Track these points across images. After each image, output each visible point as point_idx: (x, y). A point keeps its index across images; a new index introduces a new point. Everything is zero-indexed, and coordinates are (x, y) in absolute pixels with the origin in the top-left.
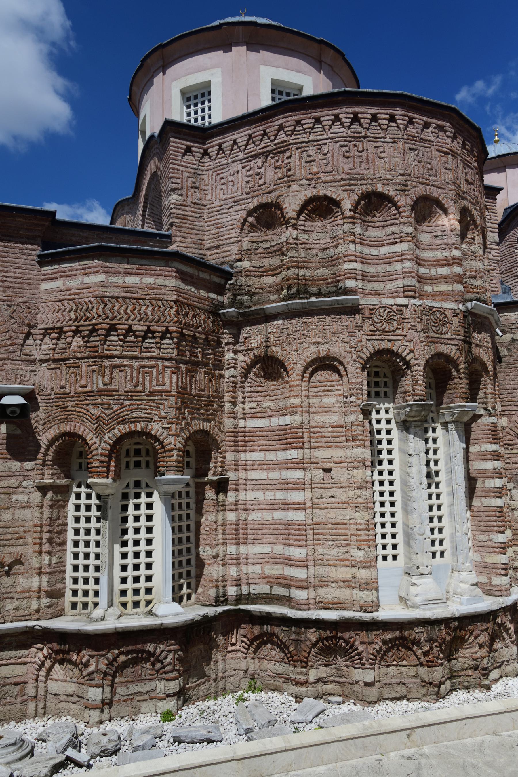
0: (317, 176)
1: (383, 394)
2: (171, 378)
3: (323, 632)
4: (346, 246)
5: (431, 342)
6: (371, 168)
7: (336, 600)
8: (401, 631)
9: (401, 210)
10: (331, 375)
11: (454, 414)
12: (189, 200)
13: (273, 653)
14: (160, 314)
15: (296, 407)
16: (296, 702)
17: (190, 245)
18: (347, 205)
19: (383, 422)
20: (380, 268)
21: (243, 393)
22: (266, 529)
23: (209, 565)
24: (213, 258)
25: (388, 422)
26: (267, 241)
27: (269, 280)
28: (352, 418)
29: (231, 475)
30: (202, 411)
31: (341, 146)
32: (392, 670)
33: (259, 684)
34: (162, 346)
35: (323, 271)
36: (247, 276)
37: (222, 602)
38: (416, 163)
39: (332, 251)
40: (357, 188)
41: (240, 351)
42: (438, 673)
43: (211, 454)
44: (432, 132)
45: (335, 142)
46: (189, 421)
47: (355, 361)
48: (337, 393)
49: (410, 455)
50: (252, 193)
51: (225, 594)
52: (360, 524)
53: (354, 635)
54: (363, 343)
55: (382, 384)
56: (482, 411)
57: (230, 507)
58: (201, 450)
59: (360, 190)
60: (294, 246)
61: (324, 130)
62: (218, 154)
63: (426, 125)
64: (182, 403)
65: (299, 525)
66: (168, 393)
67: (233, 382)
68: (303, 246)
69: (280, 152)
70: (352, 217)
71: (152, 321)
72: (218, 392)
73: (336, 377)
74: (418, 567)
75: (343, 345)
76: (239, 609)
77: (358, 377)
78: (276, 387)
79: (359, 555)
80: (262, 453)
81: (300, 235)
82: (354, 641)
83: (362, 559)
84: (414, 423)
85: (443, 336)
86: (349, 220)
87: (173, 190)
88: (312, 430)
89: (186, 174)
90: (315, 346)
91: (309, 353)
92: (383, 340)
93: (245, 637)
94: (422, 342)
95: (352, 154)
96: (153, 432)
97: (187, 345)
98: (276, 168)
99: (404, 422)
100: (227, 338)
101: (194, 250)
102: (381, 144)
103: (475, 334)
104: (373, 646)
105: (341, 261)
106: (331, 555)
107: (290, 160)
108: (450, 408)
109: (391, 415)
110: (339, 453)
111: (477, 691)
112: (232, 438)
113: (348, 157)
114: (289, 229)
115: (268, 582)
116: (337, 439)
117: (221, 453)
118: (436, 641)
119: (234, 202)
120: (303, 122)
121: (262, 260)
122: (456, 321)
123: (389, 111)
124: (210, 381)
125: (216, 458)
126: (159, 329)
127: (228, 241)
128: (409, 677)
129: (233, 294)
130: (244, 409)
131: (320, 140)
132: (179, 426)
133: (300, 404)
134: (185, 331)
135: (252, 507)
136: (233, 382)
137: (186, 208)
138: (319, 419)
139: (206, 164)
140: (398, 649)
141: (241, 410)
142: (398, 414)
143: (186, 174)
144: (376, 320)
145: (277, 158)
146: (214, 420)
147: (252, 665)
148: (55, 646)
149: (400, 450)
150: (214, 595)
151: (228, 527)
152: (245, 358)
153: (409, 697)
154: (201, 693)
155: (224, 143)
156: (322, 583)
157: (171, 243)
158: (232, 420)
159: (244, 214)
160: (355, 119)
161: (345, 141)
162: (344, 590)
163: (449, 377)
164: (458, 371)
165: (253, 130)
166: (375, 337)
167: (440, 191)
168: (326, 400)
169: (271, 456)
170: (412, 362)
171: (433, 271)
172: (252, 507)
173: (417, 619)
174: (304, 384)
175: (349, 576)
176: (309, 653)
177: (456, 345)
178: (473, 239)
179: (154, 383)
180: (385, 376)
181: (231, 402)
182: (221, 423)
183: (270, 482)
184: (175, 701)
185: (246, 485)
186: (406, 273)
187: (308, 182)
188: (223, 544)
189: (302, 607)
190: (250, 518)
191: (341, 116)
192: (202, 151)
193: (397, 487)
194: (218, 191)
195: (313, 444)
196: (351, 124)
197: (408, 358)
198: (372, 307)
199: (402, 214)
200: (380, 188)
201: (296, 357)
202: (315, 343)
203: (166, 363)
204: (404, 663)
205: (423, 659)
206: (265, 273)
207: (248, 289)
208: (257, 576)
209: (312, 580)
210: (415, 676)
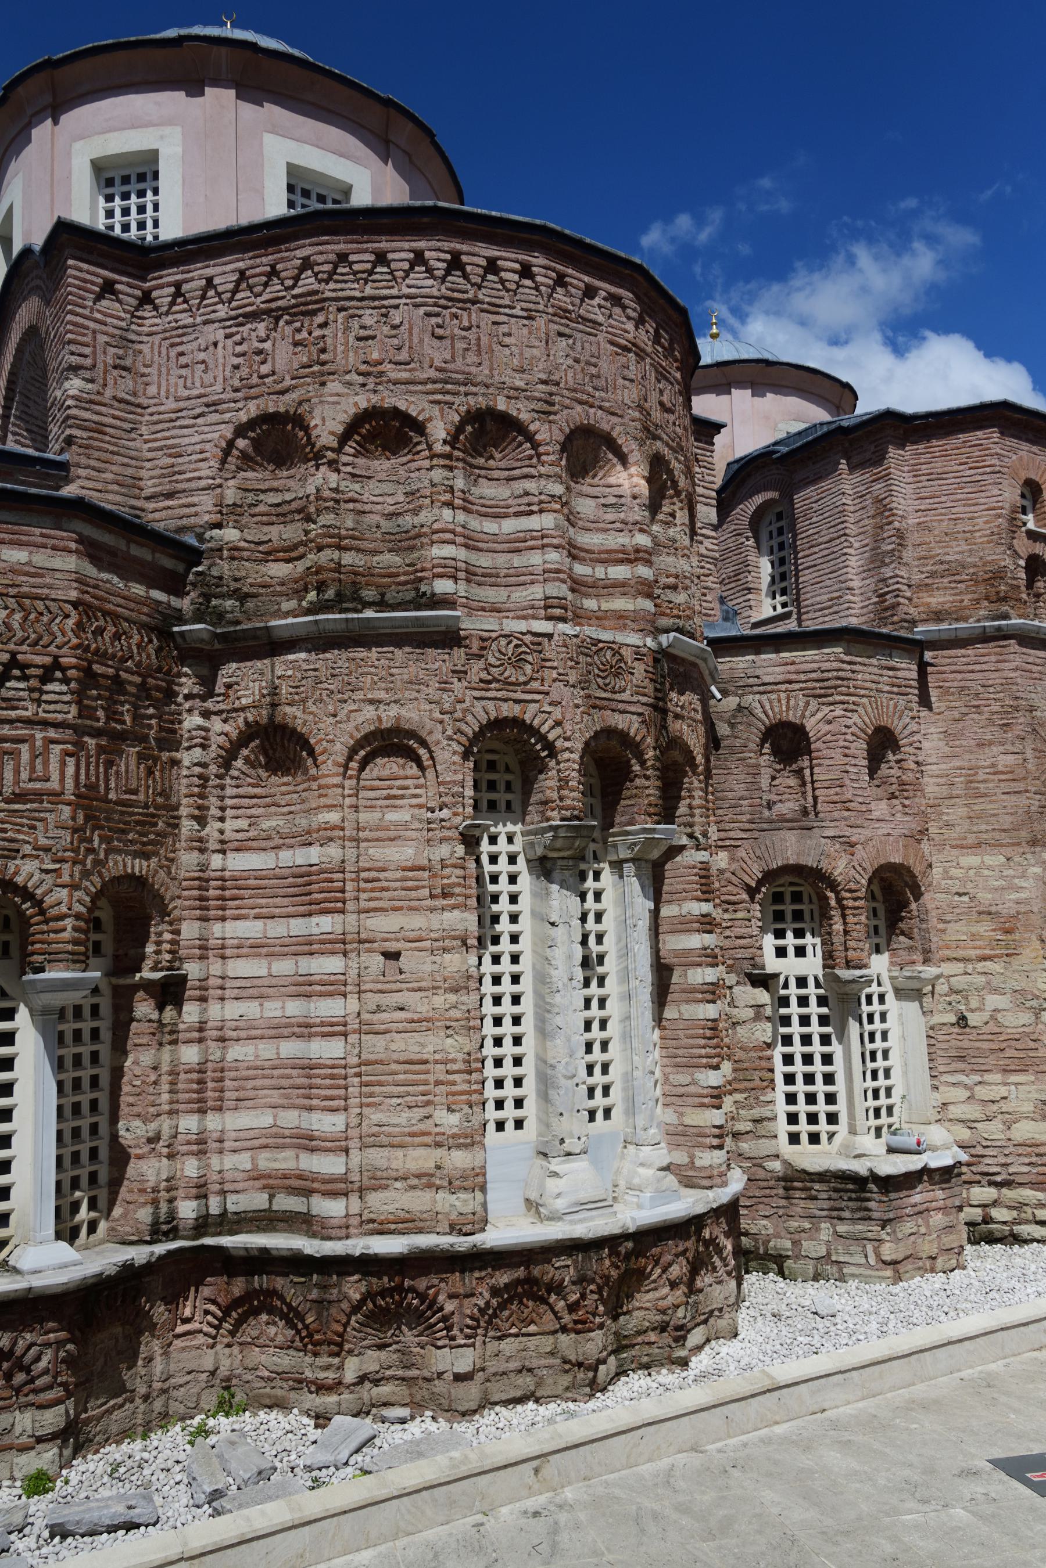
0: (380, 368)
1: (502, 806)
2: (63, 764)
3: (374, 1280)
4: (436, 511)
5: (594, 707)
6: (486, 363)
7: (402, 1214)
8: (527, 1268)
9: (541, 449)
10: (403, 767)
11: (635, 844)
12: (109, 393)
13: (272, 1330)
14: (40, 629)
15: (332, 829)
16: (316, 1426)
17: (110, 487)
18: (438, 432)
19: (503, 860)
20: (501, 560)
21: (222, 798)
22: (264, 1077)
23: (139, 1157)
24: (161, 517)
25: (512, 859)
26: (277, 490)
27: (279, 570)
28: (444, 850)
29: (192, 969)
30: (130, 836)
31: (428, 315)
32: (508, 1346)
33: (240, 1397)
34: (45, 697)
35: (389, 559)
36: (233, 558)
37: (166, 1234)
38: (570, 362)
39: (408, 521)
40: (457, 400)
41: (216, 713)
42: (594, 1343)
43: (149, 926)
44: (600, 306)
45: (417, 306)
46: (102, 855)
47: (450, 739)
48: (415, 801)
49: (553, 924)
50: (245, 390)
51: (172, 1216)
52: (454, 1061)
53: (436, 1281)
54: (467, 704)
55: (502, 787)
56: (684, 840)
57: (188, 1035)
58: (126, 916)
59: (464, 403)
60: (331, 504)
61: (395, 279)
62: (173, 303)
63: (590, 292)
64: (87, 818)
65: (333, 1067)
66: (56, 796)
67: (200, 776)
68: (351, 506)
69: (304, 314)
70: (448, 456)
71: (22, 643)
72: (168, 797)
73: (412, 769)
74: (562, 1141)
75: (428, 707)
76: (203, 1246)
77: (455, 772)
78: (291, 788)
79: (450, 1121)
80: (259, 924)
81: (343, 484)
82: (437, 1294)
83: (455, 1130)
84: (560, 863)
85: (617, 696)
86: (442, 462)
87: (75, 369)
88: (363, 875)
89: (102, 339)
90: (372, 708)
91: (360, 720)
92: (506, 700)
93: (214, 1302)
94: (577, 706)
95: (448, 332)
96: (19, 880)
97: (99, 697)
98: (296, 344)
99: (543, 859)
100: (187, 684)
101: (118, 498)
102: (505, 319)
103: (673, 695)
104: (474, 1300)
105: (425, 540)
106: (395, 1126)
107: (325, 332)
108: (627, 833)
109: (517, 847)
110: (416, 922)
111: (664, 1371)
112: (196, 893)
113: (440, 338)
114: (323, 469)
115: (265, 1187)
116: (414, 894)
117: (171, 924)
118: (593, 1281)
119: (208, 406)
120: (352, 258)
121: (266, 529)
122: (640, 668)
123: (520, 257)
124: (150, 772)
125: (160, 934)
126: (38, 660)
127: (194, 485)
128: (541, 1356)
129: (202, 594)
130: (222, 832)
131: (386, 298)
132: (78, 868)
133: (339, 823)
134: (95, 667)
135: (234, 1034)
136: (200, 776)
137: (103, 409)
138: (378, 853)
139: (147, 322)
140: (521, 1302)
141: (216, 834)
142: (532, 844)
143: (102, 339)
144: (492, 660)
145: (298, 324)
146: (156, 854)
147: (225, 1358)
149: (534, 914)
150: (149, 1220)
151: (182, 1076)
152: (227, 728)
153: (538, 1394)
154: (114, 1428)
155: (186, 281)
156: (376, 1181)
157: (68, 480)
158: (195, 854)
159: (228, 431)
160: (455, 264)
161: (436, 305)
162: (419, 1193)
163: (625, 774)
164: (642, 763)
165: (249, 263)
166: (489, 694)
167: (615, 419)
168: (392, 816)
169: (277, 929)
170: (558, 744)
171: (600, 572)
172: (234, 1034)
173: (558, 1241)
174: (348, 783)
175: (429, 1165)
176: (345, 1325)
177: (640, 714)
178: (673, 515)
179: (24, 775)
180: (508, 769)
181: (194, 817)
182: (172, 860)
183: (274, 981)
184: (56, 1450)
185: (222, 988)
186: (550, 571)
187: (360, 379)
188: (170, 1113)
189: (333, 1233)
190: (230, 1057)
191: (427, 254)
192: (139, 293)
193: (526, 985)
194: (173, 380)
195: (363, 904)
196: (448, 272)
197: (551, 736)
198: (485, 634)
199: (544, 458)
200: (501, 405)
201: (333, 729)
202: (371, 702)
203: (52, 733)
204: (532, 1328)
205: (567, 1319)
206: (271, 555)
207: (234, 585)
208: (240, 1176)
209: (355, 1178)
210: (552, 1354)
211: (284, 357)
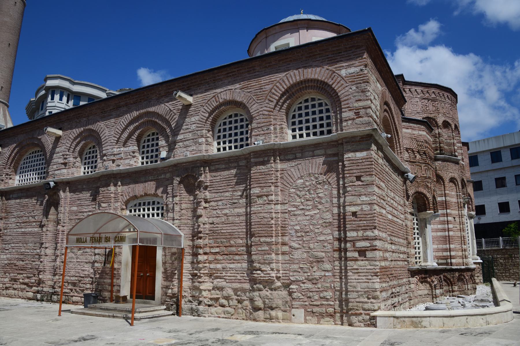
148: (423, 276)
211: (431, 108)
